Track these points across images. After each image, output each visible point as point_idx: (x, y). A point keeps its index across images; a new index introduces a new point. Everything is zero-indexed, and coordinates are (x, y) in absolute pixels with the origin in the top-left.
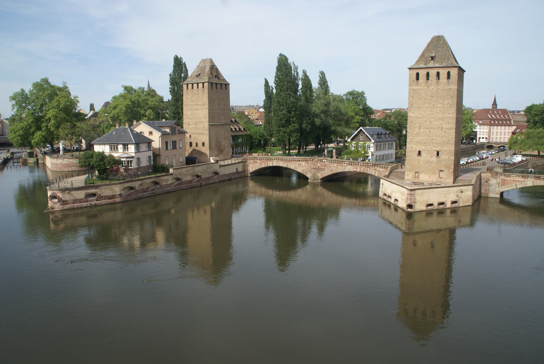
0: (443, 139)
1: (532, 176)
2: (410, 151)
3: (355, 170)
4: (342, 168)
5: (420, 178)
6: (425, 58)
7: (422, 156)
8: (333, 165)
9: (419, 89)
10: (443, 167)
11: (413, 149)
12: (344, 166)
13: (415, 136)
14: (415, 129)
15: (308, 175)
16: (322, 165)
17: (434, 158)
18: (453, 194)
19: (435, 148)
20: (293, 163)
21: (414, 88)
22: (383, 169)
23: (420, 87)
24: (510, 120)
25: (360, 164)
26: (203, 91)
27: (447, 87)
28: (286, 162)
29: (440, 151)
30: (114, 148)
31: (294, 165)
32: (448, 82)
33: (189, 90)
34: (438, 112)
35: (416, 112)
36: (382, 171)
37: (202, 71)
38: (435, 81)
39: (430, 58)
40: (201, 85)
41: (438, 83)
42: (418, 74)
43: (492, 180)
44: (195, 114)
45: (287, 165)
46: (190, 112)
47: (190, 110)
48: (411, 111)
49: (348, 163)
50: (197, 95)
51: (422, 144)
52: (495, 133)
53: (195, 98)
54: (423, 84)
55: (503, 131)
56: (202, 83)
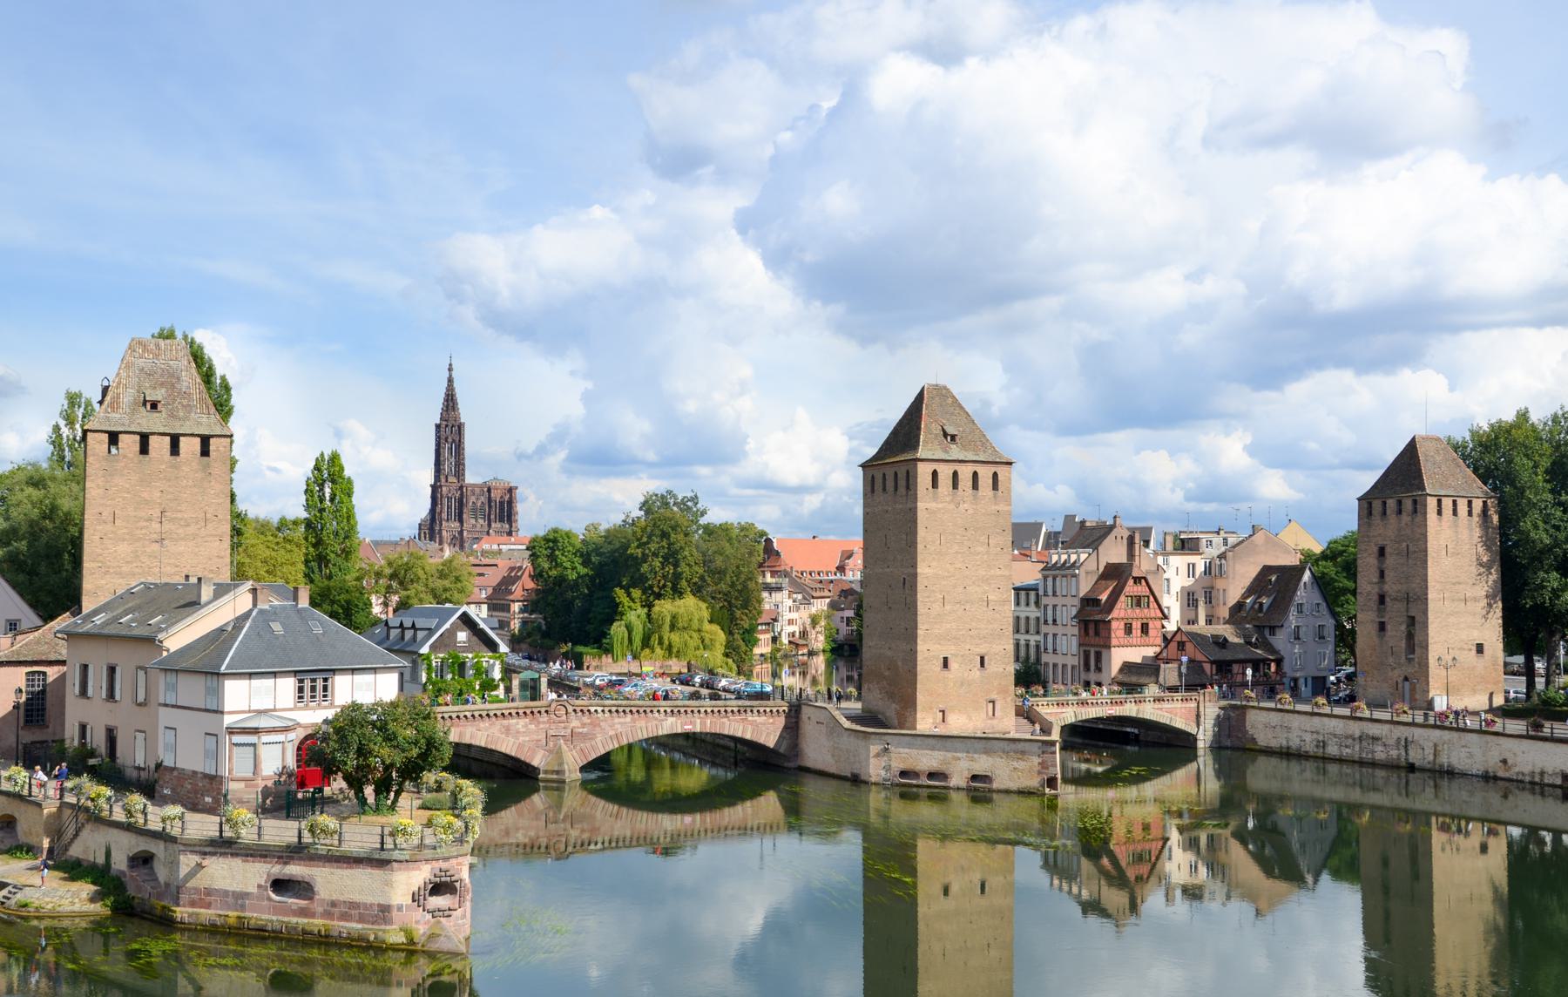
2: (925, 658)
3: (690, 727)
4: (650, 724)
6: (936, 435)
8: (622, 720)
9: (939, 509)
12: (656, 719)
13: (936, 623)
15: (537, 760)
16: (584, 725)
17: (977, 673)
20: (485, 724)
21: (928, 505)
23: (940, 506)
25: (702, 710)
26: (208, 466)
28: (458, 726)
30: (313, 689)
31: (486, 730)
32: (995, 496)
33: (125, 457)
35: (934, 564)
36: (761, 723)
37: (162, 385)
38: (970, 491)
39: (949, 438)
40: (189, 446)
41: (975, 497)
42: (935, 474)
44: (156, 557)
45: (461, 735)
46: (123, 549)
47: (124, 540)
48: (924, 561)
49: (669, 710)
50: (169, 480)
53: (159, 494)
54: (948, 499)
56: (198, 435)
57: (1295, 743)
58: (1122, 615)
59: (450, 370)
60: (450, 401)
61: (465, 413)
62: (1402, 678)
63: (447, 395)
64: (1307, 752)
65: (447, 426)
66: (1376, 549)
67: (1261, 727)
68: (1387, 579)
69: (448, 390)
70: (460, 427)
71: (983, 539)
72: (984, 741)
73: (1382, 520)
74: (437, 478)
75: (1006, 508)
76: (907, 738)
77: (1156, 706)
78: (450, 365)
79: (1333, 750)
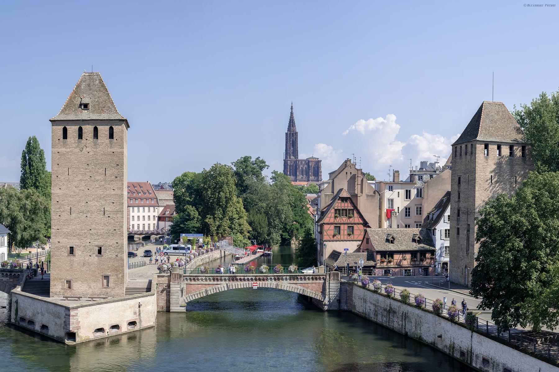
0: (106, 228)
1: (261, 276)
5: (75, 289)
7: (76, 254)
10: (109, 271)
11: (61, 245)
14: (63, 213)
17: (95, 258)
18: (130, 310)
19: (95, 243)
22: (7, 278)
24: (157, 198)
27: (109, 150)
29: (103, 246)
34: (97, 186)
35: (64, 187)
36: (5, 281)
43: (174, 286)
48: (55, 185)
51: (74, 236)
52: (136, 218)
55: (146, 214)
57: (367, 311)
58: (332, 220)
59: (292, 108)
60: (292, 123)
61: (299, 128)
62: (464, 266)
63: (290, 120)
64: (371, 318)
65: (290, 134)
66: (457, 178)
67: (357, 298)
68: (461, 199)
69: (291, 117)
70: (296, 133)
71: (102, 171)
72: (46, 303)
73: (460, 160)
74: (286, 157)
75: (120, 150)
76: (22, 298)
77: (292, 281)
78: (292, 107)
79: (380, 319)
